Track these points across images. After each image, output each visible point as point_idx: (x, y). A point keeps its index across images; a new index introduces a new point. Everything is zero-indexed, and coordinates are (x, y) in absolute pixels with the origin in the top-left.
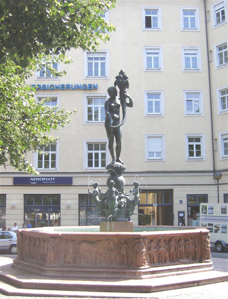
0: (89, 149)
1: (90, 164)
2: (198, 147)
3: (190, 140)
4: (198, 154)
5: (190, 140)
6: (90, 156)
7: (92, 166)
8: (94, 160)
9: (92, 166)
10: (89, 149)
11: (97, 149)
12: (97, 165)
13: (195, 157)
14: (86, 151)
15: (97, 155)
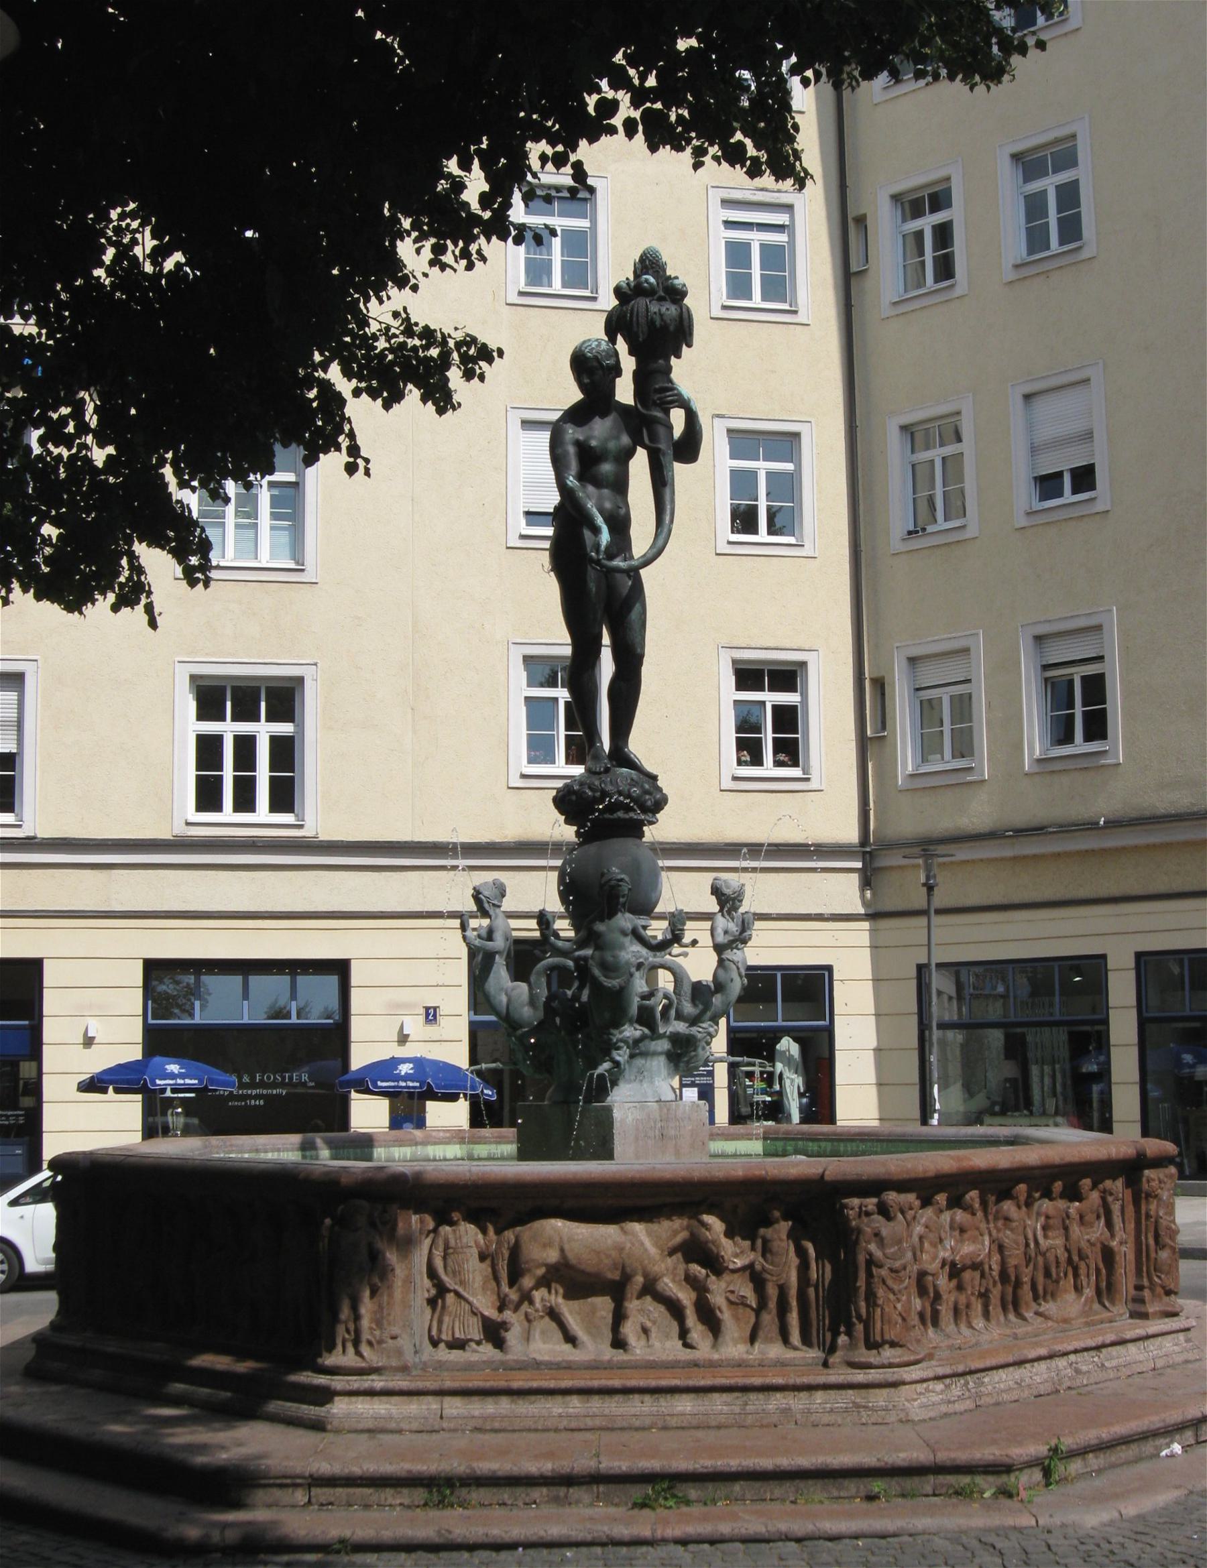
0: (202, 716)
1: (208, 797)
2: (787, 718)
3: (748, 677)
4: (789, 752)
5: (748, 677)
6: (208, 749)
7: (217, 806)
8: (228, 773)
9: (217, 806)
10: (202, 716)
11: (245, 712)
12: (245, 801)
13: (769, 769)
14: (191, 727)
15: (245, 746)
